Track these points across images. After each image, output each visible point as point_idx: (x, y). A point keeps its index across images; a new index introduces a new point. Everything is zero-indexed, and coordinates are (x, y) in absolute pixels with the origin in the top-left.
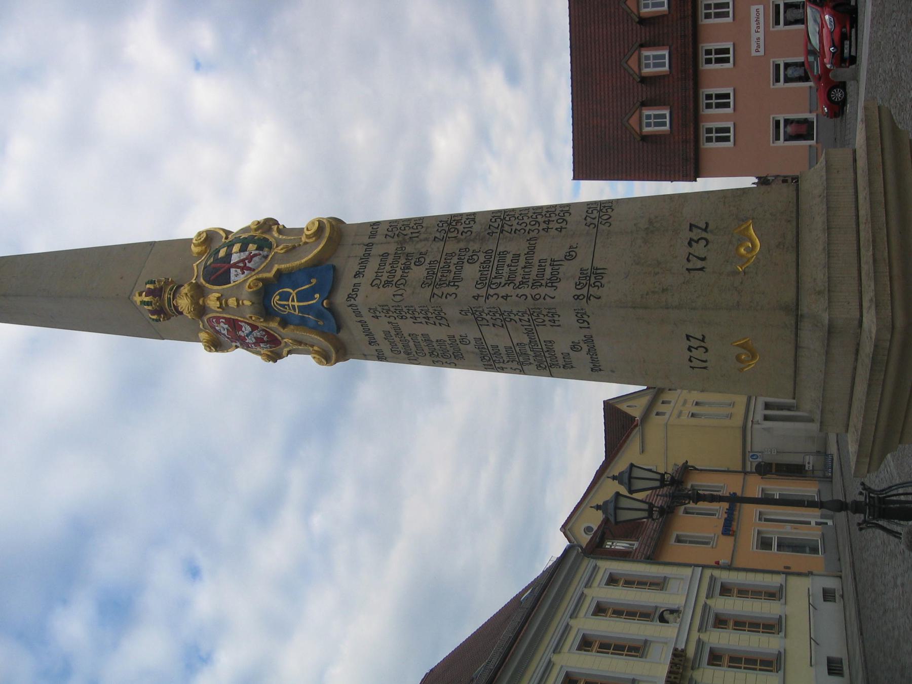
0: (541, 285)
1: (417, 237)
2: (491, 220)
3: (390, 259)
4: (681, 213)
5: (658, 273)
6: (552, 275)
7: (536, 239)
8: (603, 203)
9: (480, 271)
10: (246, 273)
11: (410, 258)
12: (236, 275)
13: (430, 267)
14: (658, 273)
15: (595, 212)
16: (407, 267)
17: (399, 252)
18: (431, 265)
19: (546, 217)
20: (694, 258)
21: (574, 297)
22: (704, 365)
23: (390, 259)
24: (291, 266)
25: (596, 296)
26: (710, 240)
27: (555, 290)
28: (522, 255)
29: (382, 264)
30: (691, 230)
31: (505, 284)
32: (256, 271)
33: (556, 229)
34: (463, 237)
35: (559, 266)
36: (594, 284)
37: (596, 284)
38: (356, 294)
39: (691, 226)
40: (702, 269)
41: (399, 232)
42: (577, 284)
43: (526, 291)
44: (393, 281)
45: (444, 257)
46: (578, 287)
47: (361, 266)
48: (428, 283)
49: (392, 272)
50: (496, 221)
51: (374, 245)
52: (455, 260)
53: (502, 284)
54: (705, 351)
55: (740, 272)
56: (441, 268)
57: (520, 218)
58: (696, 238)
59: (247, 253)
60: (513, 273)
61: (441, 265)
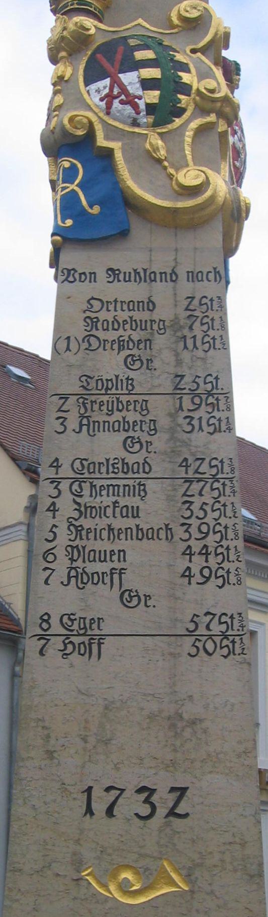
0: (72, 560)
1: (186, 347)
2: (216, 458)
3: (145, 315)
4: (211, 772)
5: (86, 742)
6: (93, 574)
7: (170, 538)
8: (241, 639)
9: (108, 460)
10: (101, 103)
11: (142, 346)
12: (98, 91)
13: (122, 380)
14: (86, 742)
15: (223, 627)
16: (121, 345)
17: (155, 327)
19: (216, 548)
20: (114, 799)
21: (46, 614)
23: (145, 315)
24: (120, 166)
25: (45, 649)
26: (149, 821)
27: (62, 583)
28: (137, 521)
29: (131, 305)
30: (173, 789)
31: (79, 504)
32: (106, 118)
33: (189, 568)
34: (180, 420)
35: (109, 583)
36: (71, 642)
37: (70, 647)
38: (75, 280)
39: (183, 791)
40: (89, 811)
41: (197, 317)
42: (72, 617)
43: (64, 537)
44: (97, 329)
45: (140, 398)
46: (65, 619)
48: (88, 384)
49: (116, 324)
50: (211, 467)
51: (171, 284)
52: (131, 417)
53: (78, 500)
55: (80, 872)
56: (118, 399)
57: (217, 506)
58: (155, 798)
59: (140, 92)
60: (102, 512)
61: (124, 399)
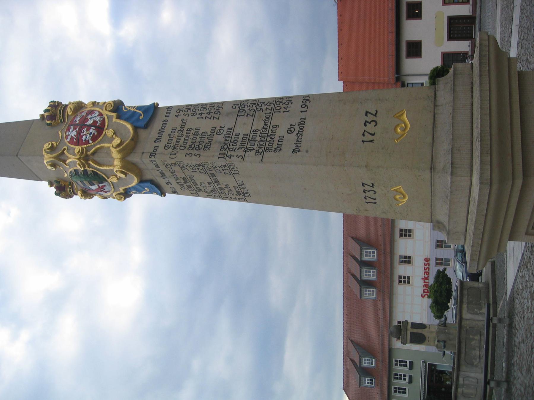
18: (202, 135)
22: (374, 201)
47: (159, 135)
54: (374, 192)
